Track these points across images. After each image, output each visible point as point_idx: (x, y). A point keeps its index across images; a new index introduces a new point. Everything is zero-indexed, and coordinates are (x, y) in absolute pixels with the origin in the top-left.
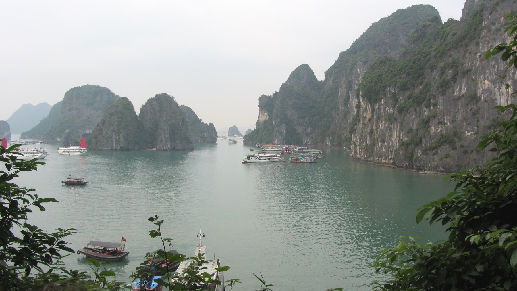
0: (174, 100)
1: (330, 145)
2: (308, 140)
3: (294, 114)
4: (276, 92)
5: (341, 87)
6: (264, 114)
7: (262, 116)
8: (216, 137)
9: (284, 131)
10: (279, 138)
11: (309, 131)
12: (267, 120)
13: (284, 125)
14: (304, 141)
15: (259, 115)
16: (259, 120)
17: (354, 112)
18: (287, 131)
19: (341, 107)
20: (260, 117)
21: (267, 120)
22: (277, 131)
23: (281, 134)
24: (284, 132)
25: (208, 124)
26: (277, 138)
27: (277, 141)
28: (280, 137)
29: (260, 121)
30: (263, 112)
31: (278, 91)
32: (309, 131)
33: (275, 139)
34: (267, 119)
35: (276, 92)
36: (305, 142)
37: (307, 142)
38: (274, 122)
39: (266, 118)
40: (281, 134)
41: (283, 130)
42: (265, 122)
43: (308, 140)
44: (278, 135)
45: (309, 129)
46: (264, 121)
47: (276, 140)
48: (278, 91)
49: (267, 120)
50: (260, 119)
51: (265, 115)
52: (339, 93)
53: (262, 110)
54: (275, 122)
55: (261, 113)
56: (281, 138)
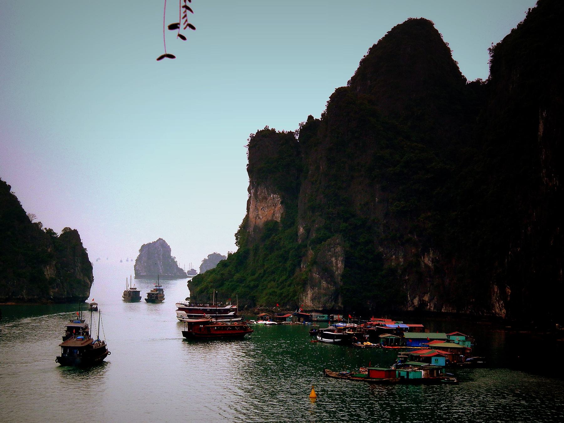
1: (503, 316)
4: (310, 117)
6: (265, 198)
8: (88, 281)
11: (430, 264)
12: (279, 220)
13: (338, 238)
14: (412, 301)
15: (249, 202)
16: (247, 216)
18: (348, 262)
20: (251, 210)
21: (279, 220)
22: (314, 262)
23: (327, 273)
25: (59, 232)
26: (312, 287)
27: (313, 299)
28: (324, 284)
29: (252, 225)
30: (262, 191)
31: (318, 116)
32: (430, 264)
33: (305, 291)
35: (310, 117)
36: (416, 302)
37: (423, 304)
38: (301, 230)
40: (327, 273)
41: (333, 259)
43: (426, 298)
44: (316, 276)
45: (431, 255)
46: (267, 223)
47: (310, 293)
48: (318, 116)
50: (251, 215)
52: (541, 127)
54: (308, 231)
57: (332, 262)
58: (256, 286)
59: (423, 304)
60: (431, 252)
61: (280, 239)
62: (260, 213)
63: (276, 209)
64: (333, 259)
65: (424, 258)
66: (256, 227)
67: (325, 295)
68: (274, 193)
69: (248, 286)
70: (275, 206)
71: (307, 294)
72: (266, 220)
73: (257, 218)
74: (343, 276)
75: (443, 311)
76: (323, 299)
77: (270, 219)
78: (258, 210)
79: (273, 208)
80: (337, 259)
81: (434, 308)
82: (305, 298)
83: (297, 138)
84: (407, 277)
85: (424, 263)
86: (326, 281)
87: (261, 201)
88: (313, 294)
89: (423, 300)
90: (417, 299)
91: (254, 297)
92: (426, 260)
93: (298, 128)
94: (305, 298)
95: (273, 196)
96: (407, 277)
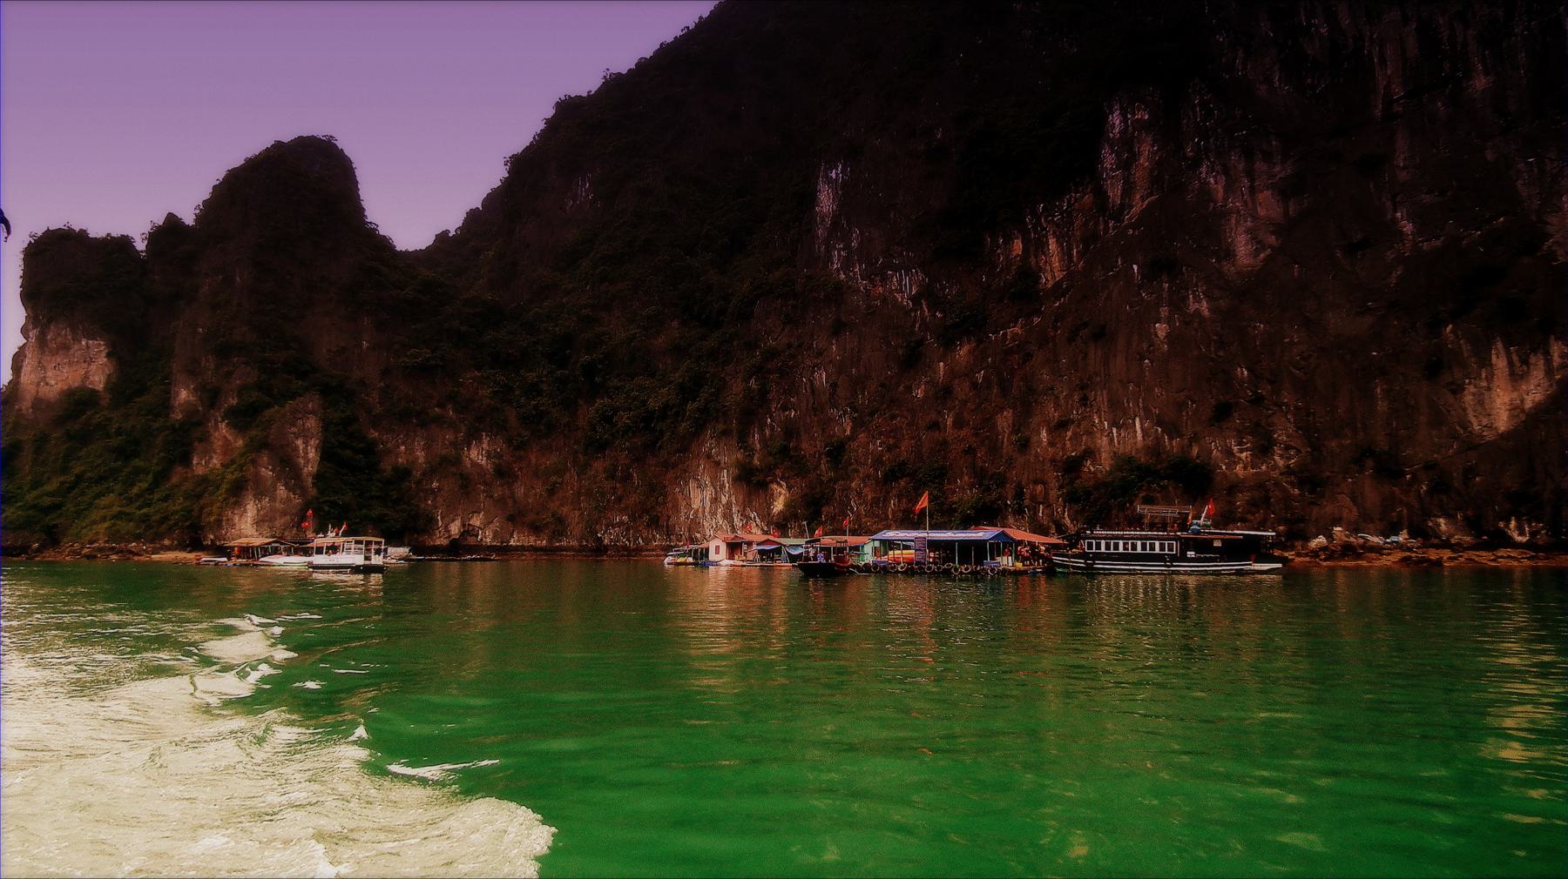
2: (476, 521)
9: (309, 455)
10: (273, 499)
12: (100, 387)
17: (1229, 254)
21: (100, 387)
24: (312, 454)
27: (258, 523)
28: (282, 491)
31: (189, 218)
37: (468, 531)
42: (79, 402)
44: (267, 473)
46: (70, 394)
49: (94, 391)
50: (27, 378)
53: (50, 321)
56: (289, 500)
57: (296, 449)
58: (56, 507)
59: (468, 531)
60: (485, 441)
61: (109, 419)
62: (49, 374)
63: (93, 367)
64: (299, 442)
65: (469, 450)
66: (38, 402)
67: (284, 513)
69: (34, 507)
70: (89, 361)
71: (245, 511)
72: (65, 388)
73: (42, 384)
74: (318, 477)
75: (512, 543)
76: (279, 523)
77: (76, 384)
78: (44, 368)
79: (85, 365)
80: (306, 443)
81: (494, 537)
82: (240, 520)
83: (141, 245)
84: (435, 485)
85: (470, 459)
86: (286, 485)
87: (54, 353)
88: (258, 511)
89: (469, 525)
90: (458, 523)
91: (55, 526)
92: (474, 454)
93: (147, 228)
94: (240, 520)
95: (87, 344)
96: (435, 485)
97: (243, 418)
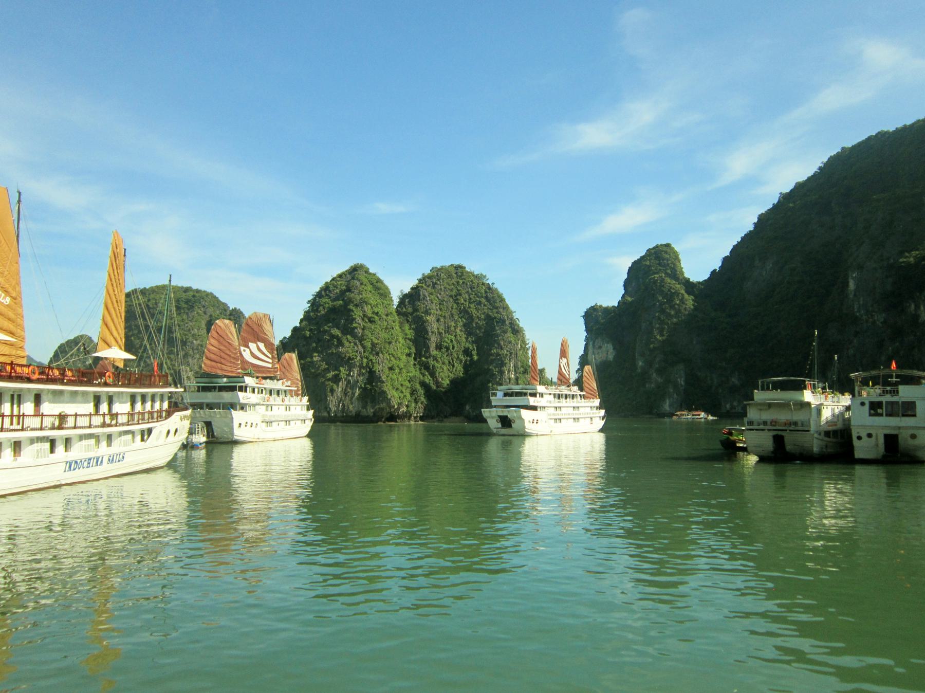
0: (490, 282)
3: (694, 342)
5: (860, 267)
6: (600, 347)
7: (596, 351)
9: (681, 381)
12: (612, 360)
19: (864, 317)
24: (683, 383)
30: (599, 342)
34: (611, 357)
36: (728, 406)
37: (732, 407)
39: (607, 357)
41: (679, 380)
47: (668, 402)
49: (610, 361)
51: (604, 349)
53: (596, 338)
55: (594, 343)
59: (732, 407)
68: (608, 343)
97: (660, 372)
